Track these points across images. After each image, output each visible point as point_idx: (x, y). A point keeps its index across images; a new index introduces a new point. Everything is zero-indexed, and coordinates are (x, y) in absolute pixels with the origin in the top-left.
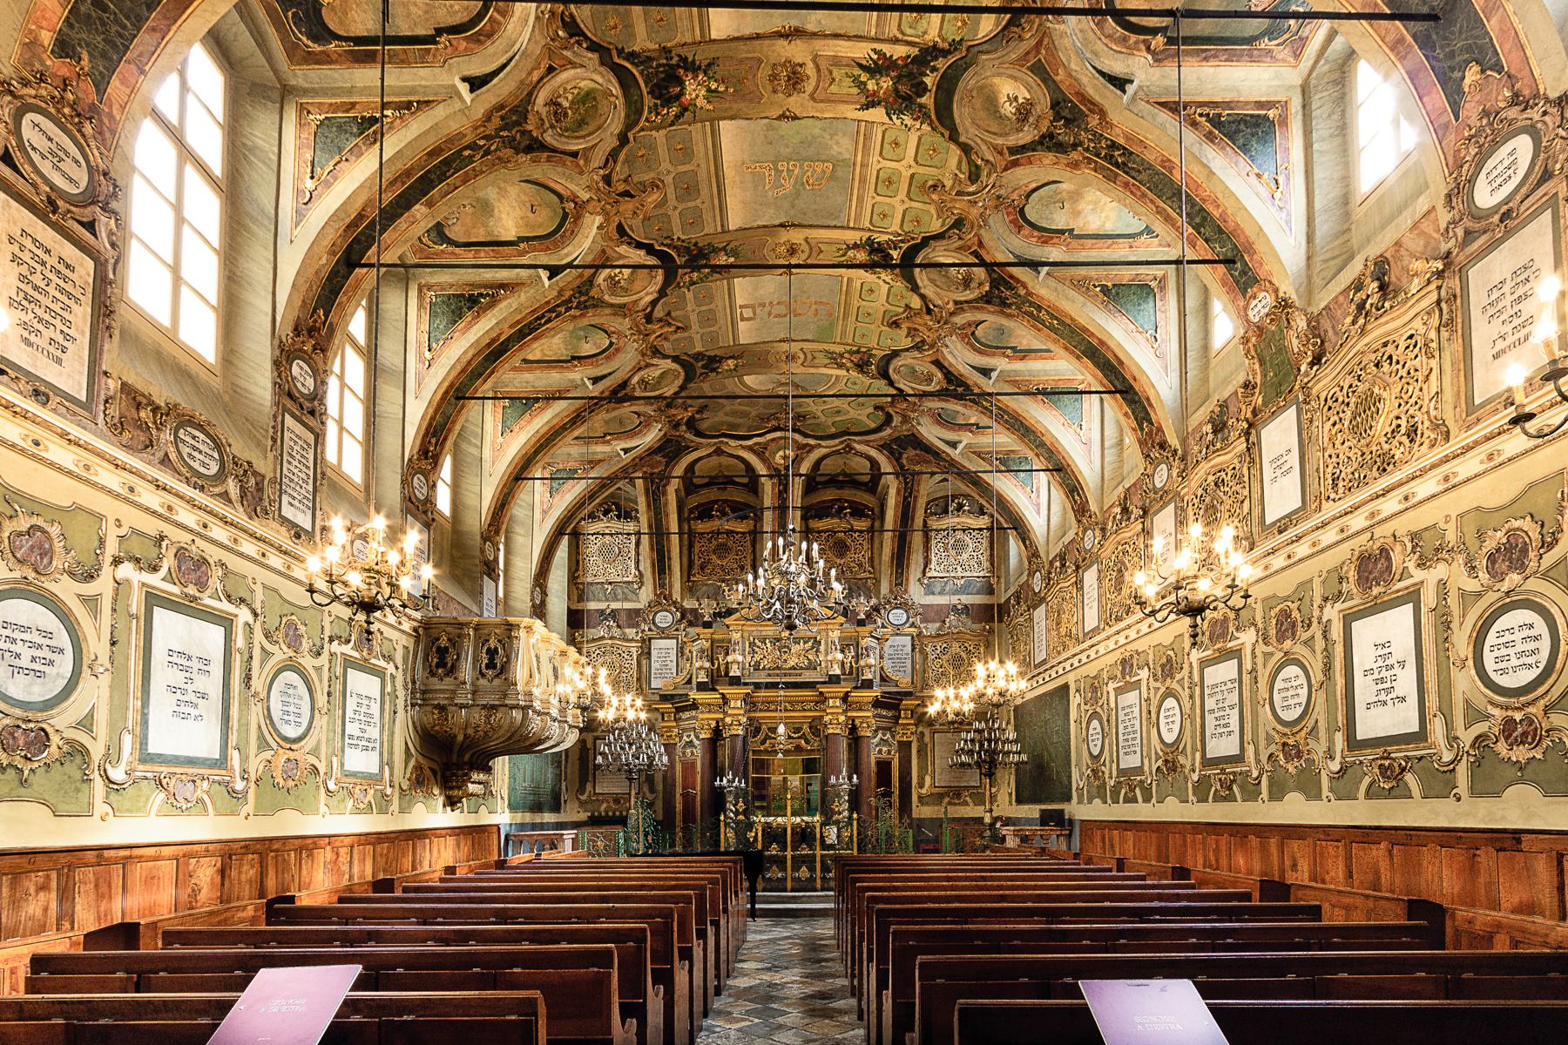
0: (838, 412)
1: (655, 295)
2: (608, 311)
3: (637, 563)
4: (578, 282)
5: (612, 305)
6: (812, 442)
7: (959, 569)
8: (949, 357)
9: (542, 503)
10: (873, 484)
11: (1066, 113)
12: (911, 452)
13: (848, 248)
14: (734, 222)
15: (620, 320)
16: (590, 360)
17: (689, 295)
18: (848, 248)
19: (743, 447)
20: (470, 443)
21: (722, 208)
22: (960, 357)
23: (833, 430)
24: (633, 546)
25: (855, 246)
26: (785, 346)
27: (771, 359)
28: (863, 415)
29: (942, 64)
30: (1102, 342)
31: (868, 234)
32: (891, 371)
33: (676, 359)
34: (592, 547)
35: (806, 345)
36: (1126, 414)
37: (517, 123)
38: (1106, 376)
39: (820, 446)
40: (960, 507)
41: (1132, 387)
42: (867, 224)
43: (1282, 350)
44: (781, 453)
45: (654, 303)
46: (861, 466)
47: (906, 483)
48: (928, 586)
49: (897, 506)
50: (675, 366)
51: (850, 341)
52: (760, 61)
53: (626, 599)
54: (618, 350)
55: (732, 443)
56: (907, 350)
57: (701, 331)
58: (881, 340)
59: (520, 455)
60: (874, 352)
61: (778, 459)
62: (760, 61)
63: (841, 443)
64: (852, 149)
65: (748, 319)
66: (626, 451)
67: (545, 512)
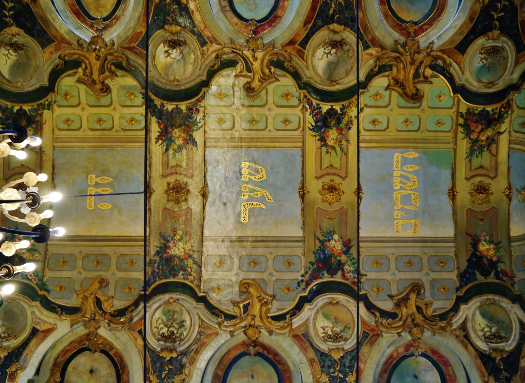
11: (161, 17)
13: (326, 145)
18: (326, 145)
25: (323, 139)
29: (158, 102)
37: (162, 365)
42: (298, 133)
52: (165, 209)
62: (165, 209)
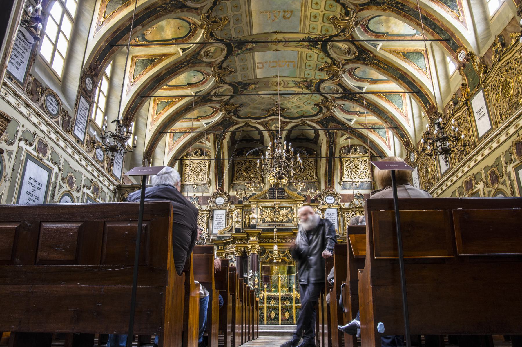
0: (299, 107)
1: (223, 59)
2: (204, 65)
3: (209, 175)
4: (193, 53)
5: (206, 62)
6: (288, 120)
7: (357, 178)
8: (344, 82)
9: (169, 146)
10: (316, 140)
12: (331, 125)
14: (255, 31)
15: (209, 68)
16: (195, 85)
17: (237, 59)
19: (258, 123)
20: (143, 118)
21: (251, 27)
22: (350, 83)
23: (297, 115)
24: (207, 168)
26: (275, 79)
27: (270, 84)
28: (310, 109)
30: (405, 73)
31: (308, 35)
32: (321, 89)
33: (230, 84)
34: (188, 169)
35: (285, 79)
36: (420, 101)
38: (409, 87)
39: (291, 122)
40: (356, 150)
41: (420, 91)
43: (473, 70)
44: (274, 125)
45: (223, 62)
46: (312, 133)
47: (331, 138)
48: (343, 185)
49: (327, 148)
50: (230, 87)
51: (303, 77)
53: (203, 192)
54: (206, 81)
55: (253, 121)
56: (327, 80)
57: (241, 73)
58: (316, 76)
59: (163, 123)
60: (313, 81)
61: (273, 127)
63: (301, 121)
64: (300, 5)
65: (261, 68)
66: (207, 124)
67: (170, 150)
